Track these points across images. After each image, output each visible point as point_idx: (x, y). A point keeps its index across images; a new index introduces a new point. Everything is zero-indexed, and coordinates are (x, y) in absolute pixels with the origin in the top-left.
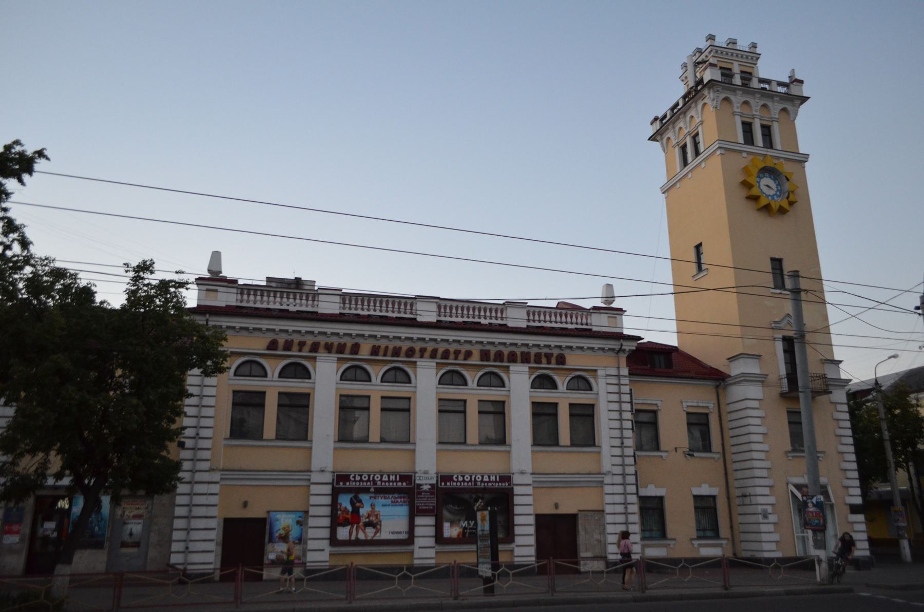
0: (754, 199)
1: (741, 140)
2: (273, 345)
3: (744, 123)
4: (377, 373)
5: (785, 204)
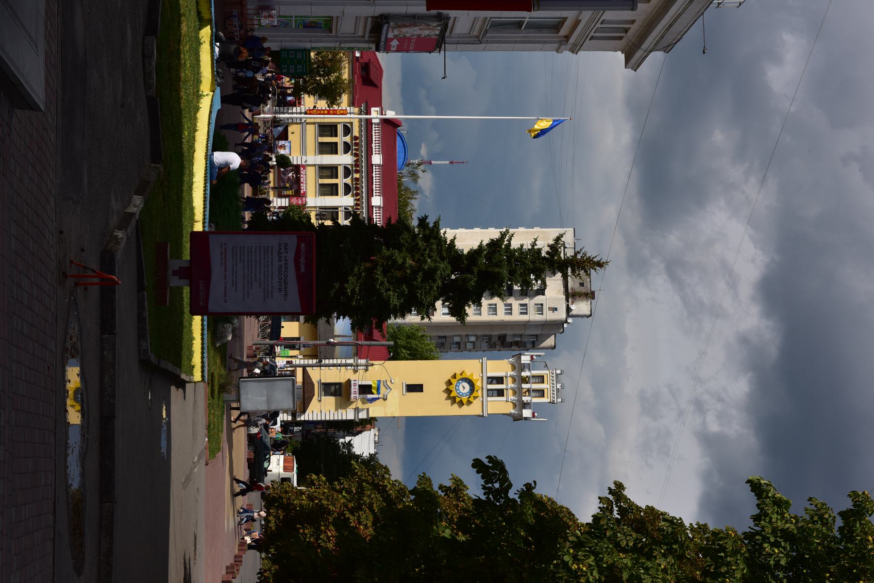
0: (454, 376)
1: (489, 375)
2: (356, 138)
3: (502, 378)
4: (348, 181)
5: (452, 395)
